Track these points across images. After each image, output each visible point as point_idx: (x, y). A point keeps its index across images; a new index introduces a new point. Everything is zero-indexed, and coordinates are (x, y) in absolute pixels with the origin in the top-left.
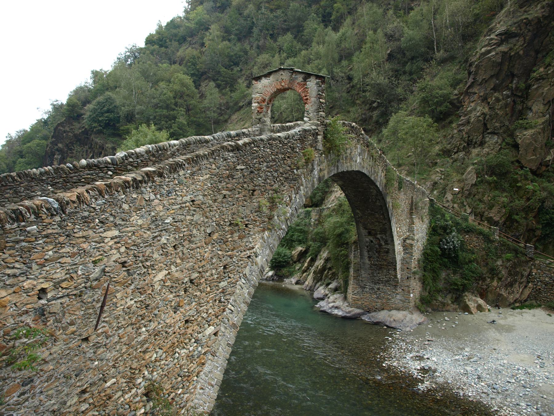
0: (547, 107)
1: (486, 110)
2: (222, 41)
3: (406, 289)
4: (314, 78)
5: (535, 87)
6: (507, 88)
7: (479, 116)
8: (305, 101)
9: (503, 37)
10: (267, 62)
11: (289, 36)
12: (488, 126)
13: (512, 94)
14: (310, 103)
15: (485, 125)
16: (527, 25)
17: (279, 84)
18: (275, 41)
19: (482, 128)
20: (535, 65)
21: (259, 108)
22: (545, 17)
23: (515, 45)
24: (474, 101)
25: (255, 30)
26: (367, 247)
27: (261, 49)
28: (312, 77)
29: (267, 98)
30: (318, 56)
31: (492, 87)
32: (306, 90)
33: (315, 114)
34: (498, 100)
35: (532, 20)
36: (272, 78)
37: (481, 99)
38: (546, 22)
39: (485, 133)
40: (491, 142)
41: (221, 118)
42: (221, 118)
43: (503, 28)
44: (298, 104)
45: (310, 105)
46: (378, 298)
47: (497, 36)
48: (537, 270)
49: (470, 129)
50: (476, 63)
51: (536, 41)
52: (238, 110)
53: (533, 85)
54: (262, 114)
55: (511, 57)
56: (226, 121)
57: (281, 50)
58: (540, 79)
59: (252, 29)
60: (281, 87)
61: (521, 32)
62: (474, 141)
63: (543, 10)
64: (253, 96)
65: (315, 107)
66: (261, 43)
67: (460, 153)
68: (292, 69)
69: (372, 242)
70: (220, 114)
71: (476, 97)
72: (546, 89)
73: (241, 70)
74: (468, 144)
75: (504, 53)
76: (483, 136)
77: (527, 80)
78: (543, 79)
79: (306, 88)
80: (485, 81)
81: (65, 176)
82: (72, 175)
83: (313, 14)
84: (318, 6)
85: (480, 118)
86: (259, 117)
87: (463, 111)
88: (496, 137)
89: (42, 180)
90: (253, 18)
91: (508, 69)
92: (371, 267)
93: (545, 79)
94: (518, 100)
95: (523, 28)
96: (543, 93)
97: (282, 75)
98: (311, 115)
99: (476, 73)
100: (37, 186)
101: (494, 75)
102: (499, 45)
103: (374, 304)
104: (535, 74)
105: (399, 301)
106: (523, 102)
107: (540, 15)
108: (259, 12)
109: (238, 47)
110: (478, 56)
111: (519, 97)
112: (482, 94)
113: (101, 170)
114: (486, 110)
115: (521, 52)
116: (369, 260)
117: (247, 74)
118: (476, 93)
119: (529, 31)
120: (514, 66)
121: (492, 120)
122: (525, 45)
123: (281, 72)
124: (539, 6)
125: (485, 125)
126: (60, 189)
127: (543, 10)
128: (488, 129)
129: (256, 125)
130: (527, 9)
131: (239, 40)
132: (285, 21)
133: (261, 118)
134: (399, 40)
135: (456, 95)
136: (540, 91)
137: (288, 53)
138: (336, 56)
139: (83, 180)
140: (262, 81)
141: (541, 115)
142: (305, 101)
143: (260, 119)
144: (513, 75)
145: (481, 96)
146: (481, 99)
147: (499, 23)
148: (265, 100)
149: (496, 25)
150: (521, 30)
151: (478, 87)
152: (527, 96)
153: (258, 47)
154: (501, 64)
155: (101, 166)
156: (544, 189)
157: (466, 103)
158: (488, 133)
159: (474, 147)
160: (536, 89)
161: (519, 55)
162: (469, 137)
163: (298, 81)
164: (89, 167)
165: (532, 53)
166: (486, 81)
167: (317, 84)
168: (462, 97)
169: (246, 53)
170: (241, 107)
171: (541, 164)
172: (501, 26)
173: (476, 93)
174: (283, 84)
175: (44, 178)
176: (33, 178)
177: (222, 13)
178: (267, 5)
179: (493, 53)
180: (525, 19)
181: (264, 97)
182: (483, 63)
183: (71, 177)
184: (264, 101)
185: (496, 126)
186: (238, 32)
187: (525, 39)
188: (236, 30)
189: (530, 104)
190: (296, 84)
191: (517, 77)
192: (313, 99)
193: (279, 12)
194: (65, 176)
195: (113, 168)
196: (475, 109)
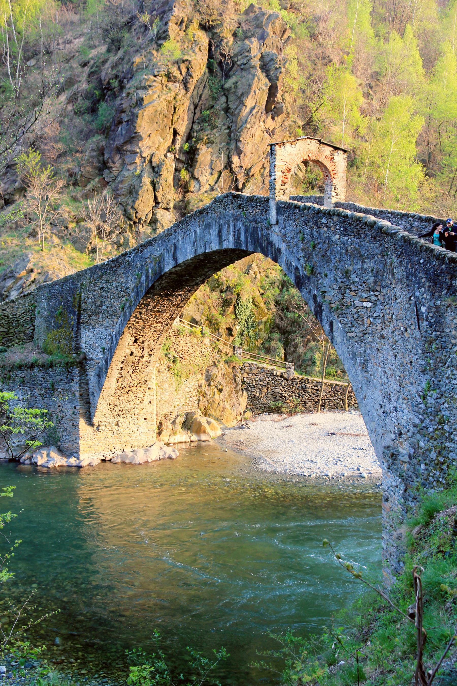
12: (159, 200)
17: (305, 154)
31: (157, 146)
48: (248, 373)
76: (153, 212)
86: (283, 187)
87: (112, 175)
157: (117, 165)
174: (310, 155)
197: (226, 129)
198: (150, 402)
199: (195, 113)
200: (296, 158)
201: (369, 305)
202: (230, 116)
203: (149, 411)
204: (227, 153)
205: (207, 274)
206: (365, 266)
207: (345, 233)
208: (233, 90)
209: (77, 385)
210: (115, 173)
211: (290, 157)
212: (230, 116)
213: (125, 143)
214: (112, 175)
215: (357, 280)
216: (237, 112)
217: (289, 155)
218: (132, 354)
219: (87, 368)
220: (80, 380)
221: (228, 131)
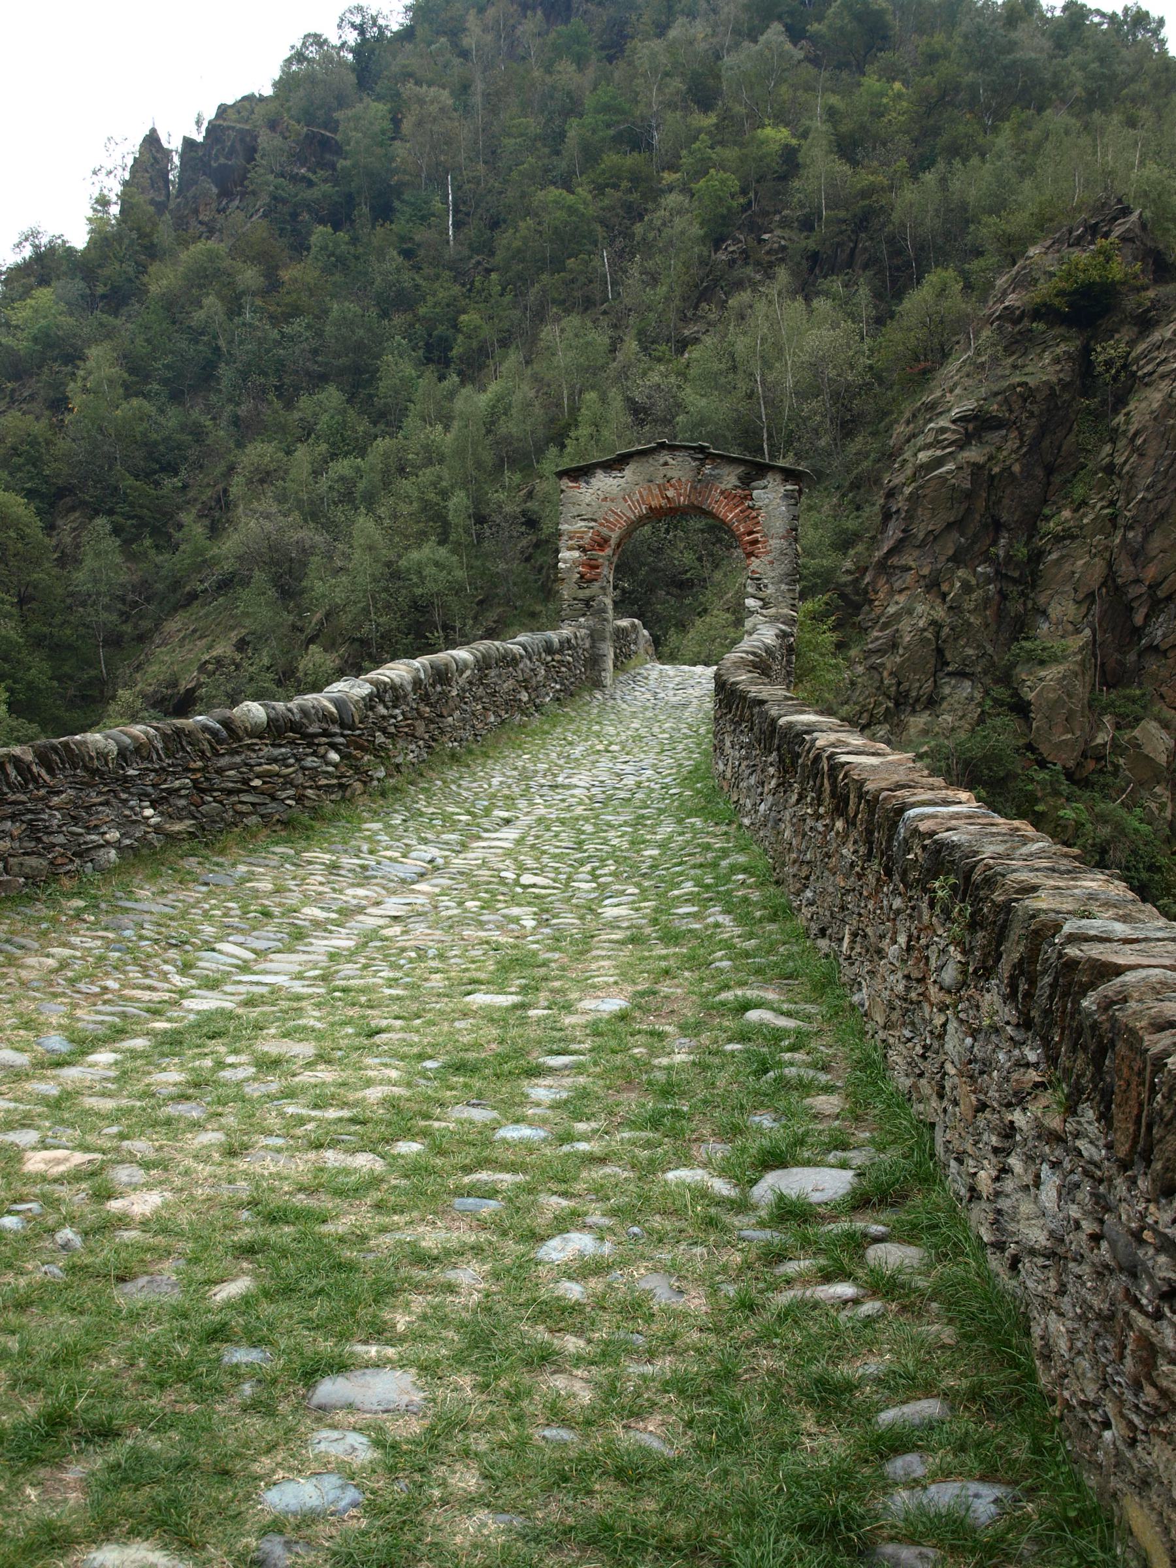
0: (1084, 610)
1: (940, 613)
2: (127, 397)
5: (1054, 556)
6: (987, 559)
7: (925, 630)
8: (749, 549)
9: (971, 427)
10: (272, 467)
11: (332, 396)
12: (948, 656)
13: (997, 572)
14: (767, 553)
15: (940, 651)
16: (1025, 400)
17: (656, 491)
18: (289, 405)
19: (933, 661)
20: (1045, 502)
21: (583, 565)
22: (1065, 386)
23: (999, 449)
24: (907, 588)
25: (226, 373)
27: (245, 430)
28: (770, 477)
29: (614, 536)
30: (432, 456)
31: (951, 552)
32: (750, 514)
33: (784, 587)
34: (967, 588)
35: (1038, 389)
36: (629, 471)
37: (922, 583)
38: (1066, 396)
39: (941, 674)
40: (956, 697)
41: (127, 628)
42: (127, 628)
43: (969, 405)
44: (386, 590)
47: (954, 422)
49: (903, 662)
50: (907, 491)
51: (1046, 443)
52: (184, 606)
54: (597, 584)
55: (992, 478)
56: (142, 638)
57: (307, 432)
58: (1064, 538)
59: (215, 367)
60: (663, 502)
61: (1013, 417)
62: (914, 694)
63: (1058, 367)
64: (564, 527)
65: (782, 568)
66: (243, 411)
67: (878, 727)
68: (702, 449)
70: (125, 617)
71: (909, 577)
72: (1080, 563)
73: (185, 487)
74: (897, 705)
75: (977, 468)
77: (1031, 537)
78: (1073, 538)
79: (752, 508)
80: (934, 537)
81: (200, 764)
82: (223, 762)
83: (398, 338)
84: (409, 316)
85: (928, 635)
87: (873, 616)
88: (967, 684)
89: (126, 779)
90: (216, 337)
91: (987, 508)
93: (1077, 537)
94: (1013, 590)
95: (1016, 407)
96: (1073, 573)
97: (666, 464)
98: (770, 590)
99: (910, 517)
100: (106, 803)
101: (954, 523)
102: (962, 445)
104: (1052, 524)
106: (1022, 594)
107: (1054, 379)
108: (237, 320)
109: (172, 419)
110: (909, 472)
111: (1015, 581)
112: (925, 571)
113: (309, 745)
114: (940, 613)
115: (1016, 468)
117: (204, 498)
118: (911, 569)
119: (1032, 415)
120: (999, 501)
121: (956, 639)
122: (1024, 450)
123: (665, 456)
124: (1047, 358)
125: (940, 651)
126: (181, 819)
127: (1058, 367)
128: (948, 664)
129: (574, 618)
130: (1020, 362)
131: (176, 397)
132: (315, 352)
133: (592, 598)
134: (668, 421)
135: (848, 572)
136: (1067, 568)
137: (334, 444)
138: (488, 458)
139: (257, 783)
140: (593, 481)
141: (1070, 628)
142: (749, 549)
143: (587, 602)
144: (997, 526)
145: (924, 577)
146: (922, 583)
147: (951, 391)
149: (943, 396)
150: (1011, 411)
151: (916, 553)
152: (1034, 581)
153: (236, 421)
154: (969, 495)
155: (311, 730)
156: (1102, 819)
157: (881, 595)
158: (949, 674)
159: (914, 712)
160: (1058, 562)
161: (1012, 474)
162: (899, 684)
163: (723, 487)
164: (277, 729)
165: (1039, 472)
166: (935, 538)
167: (788, 495)
168: (867, 579)
169: (198, 433)
170: (193, 597)
171: (1084, 755)
172: (960, 398)
173: (911, 569)
174: (671, 493)
175: (131, 772)
176: (94, 772)
177: (116, 313)
178: (259, 302)
179: (950, 466)
180: (1020, 384)
181: (605, 531)
182: (927, 491)
183: (220, 771)
184: (602, 542)
185: (969, 656)
186: (169, 374)
187: (1021, 435)
188: (166, 367)
189: (1042, 600)
190: (716, 494)
191: (1009, 531)
192: (774, 543)
193: (297, 326)
194: (200, 764)
195: (341, 740)
196: (910, 612)
199: (1049, 484)
204: (1107, 555)
208: (1123, 428)
210: (878, 611)
211: (608, 503)
212: (1118, 482)
213: (891, 552)
214: (873, 616)
216: (1127, 468)
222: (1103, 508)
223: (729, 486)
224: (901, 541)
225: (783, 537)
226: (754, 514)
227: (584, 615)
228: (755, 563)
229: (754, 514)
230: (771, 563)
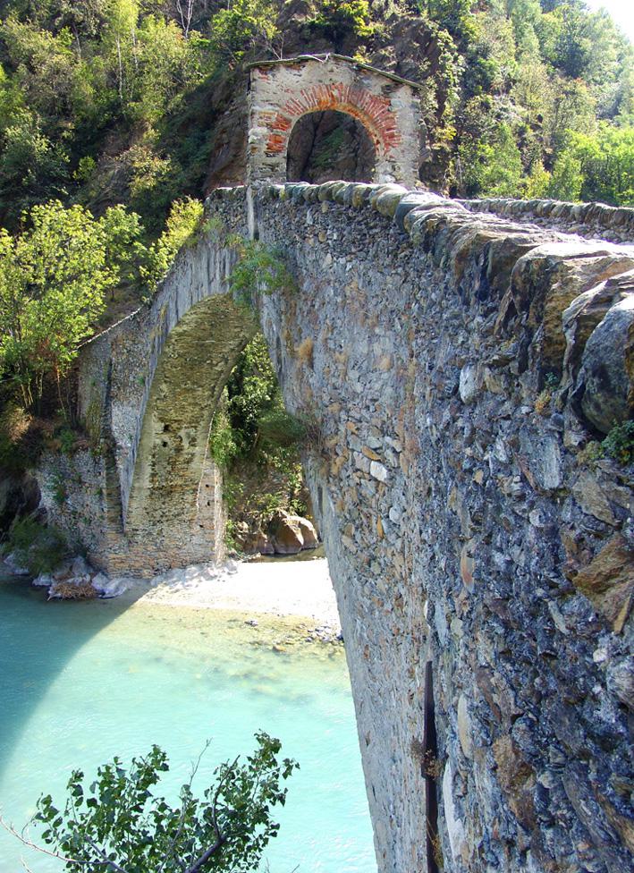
3: (206, 523)
4: (409, 91)
26: (154, 456)
29: (294, 119)
36: (304, 71)
45: (399, 148)
46: (159, 550)
53: (319, 176)
54: (281, 155)
64: (256, 108)
69: (165, 444)
86: (273, 160)
92: (152, 493)
97: (332, 71)
103: (152, 562)
105: (196, 548)
116: (152, 481)
133: (278, 165)
140: (278, 75)
143: (273, 167)
148: (288, 122)
163: (371, 93)
174: (335, 93)
181: (286, 115)
192: (405, 138)
197: (350, 153)
198: (209, 504)
199: (315, 135)
200: (300, 98)
201: (380, 472)
202: (358, 138)
203: (207, 515)
205: (241, 335)
206: (377, 348)
207: (340, 249)
209: (105, 480)
211: (289, 95)
215: (359, 388)
217: (287, 91)
218: (165, 444)
219: (117, 458)
220: (107, 474)
221: (353, 155)
222: (350, 153)
223: (376, 93)
224: (233, 162)
225: (411, 135)
226: (391, 115)
227: (270, 177)
228: (392, 151)
229: (391, 115)
230: (403, 151)
